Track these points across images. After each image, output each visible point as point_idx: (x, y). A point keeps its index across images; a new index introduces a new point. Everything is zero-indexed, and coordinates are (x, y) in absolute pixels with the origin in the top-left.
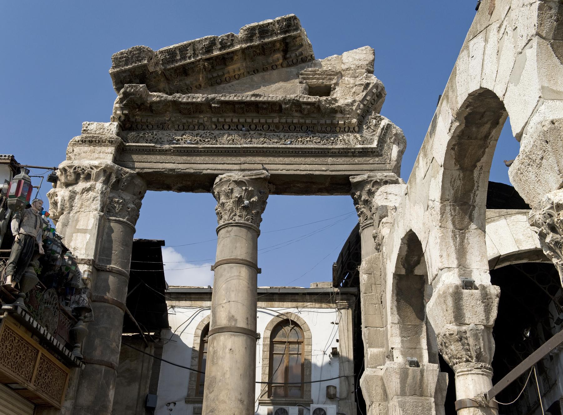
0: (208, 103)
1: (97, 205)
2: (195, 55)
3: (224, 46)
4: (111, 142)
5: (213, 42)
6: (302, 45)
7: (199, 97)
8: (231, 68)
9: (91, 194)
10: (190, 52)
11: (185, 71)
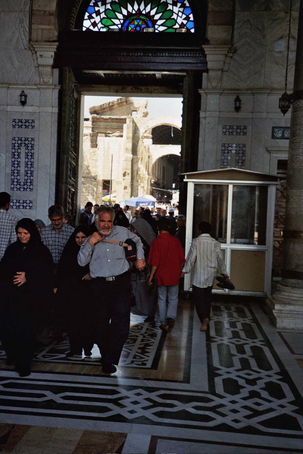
0: (110, 118)
1: (90, 141)
2: (106, 105)
3: (112, 103)
4: (90, 127)
5: (110, 103)
6: (130, 101)
7: (107, 117)
8: (114, 107)
9: (88, 139)
10: (105, 105)
11: (104, 109)
